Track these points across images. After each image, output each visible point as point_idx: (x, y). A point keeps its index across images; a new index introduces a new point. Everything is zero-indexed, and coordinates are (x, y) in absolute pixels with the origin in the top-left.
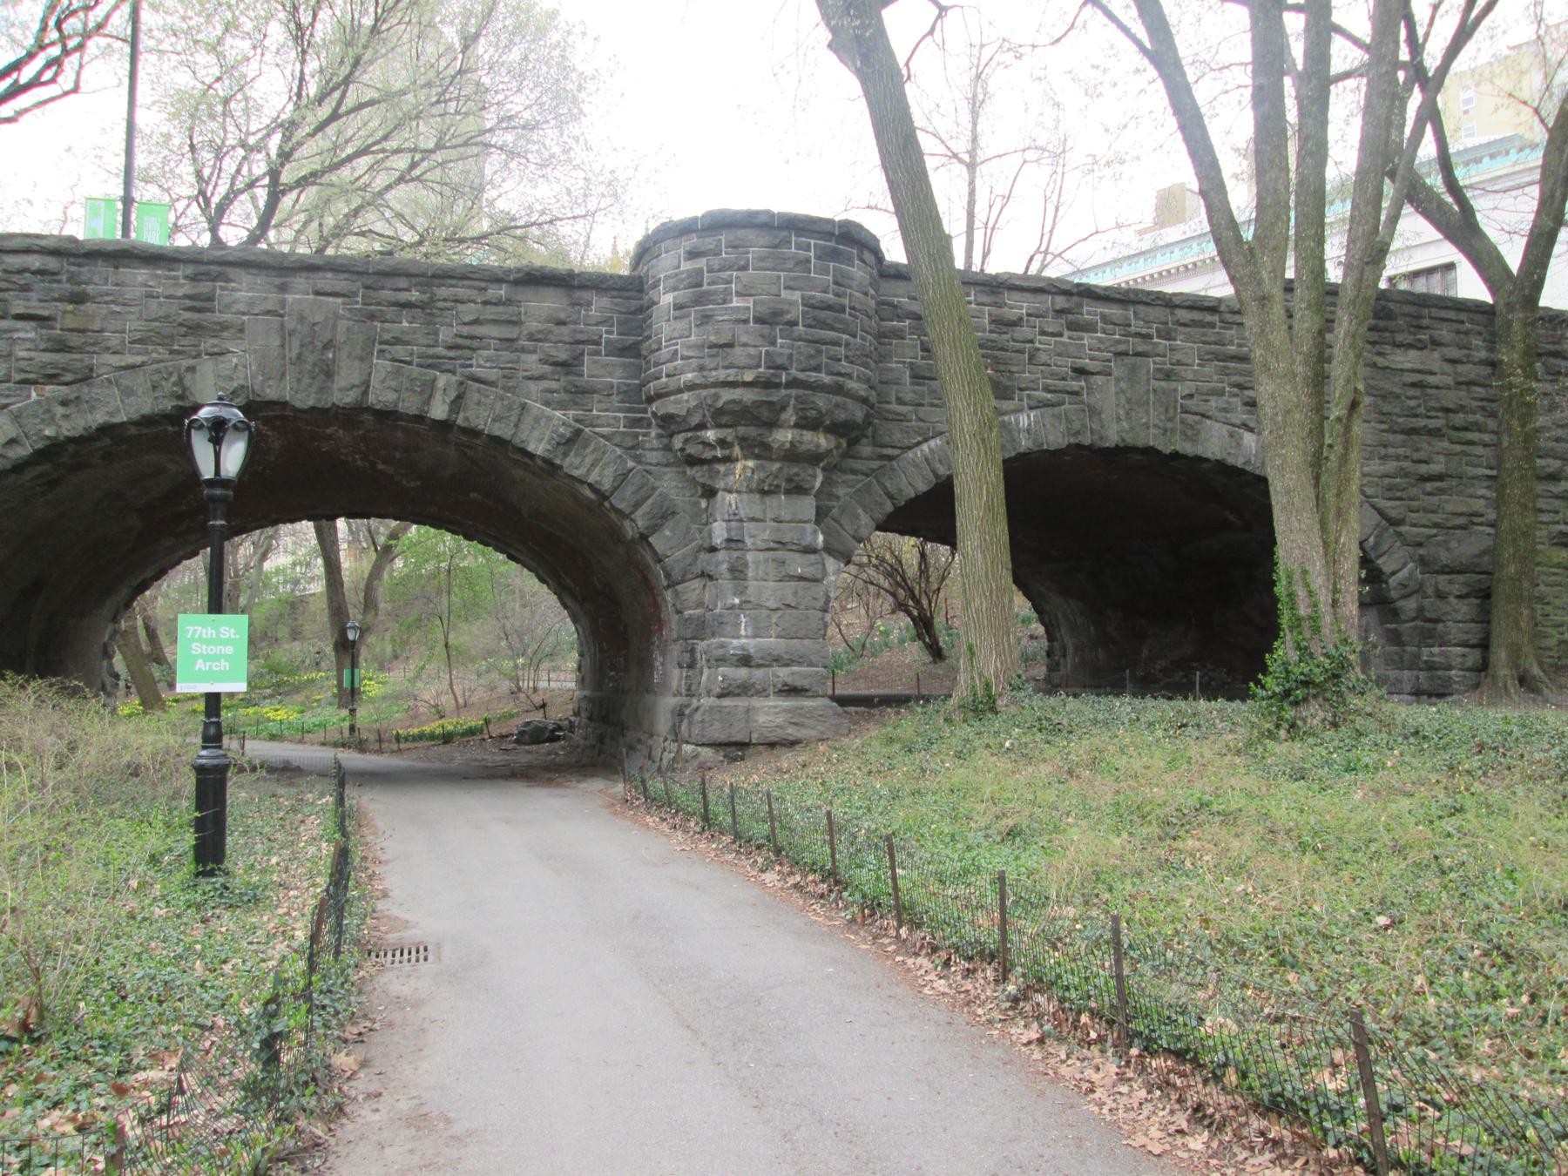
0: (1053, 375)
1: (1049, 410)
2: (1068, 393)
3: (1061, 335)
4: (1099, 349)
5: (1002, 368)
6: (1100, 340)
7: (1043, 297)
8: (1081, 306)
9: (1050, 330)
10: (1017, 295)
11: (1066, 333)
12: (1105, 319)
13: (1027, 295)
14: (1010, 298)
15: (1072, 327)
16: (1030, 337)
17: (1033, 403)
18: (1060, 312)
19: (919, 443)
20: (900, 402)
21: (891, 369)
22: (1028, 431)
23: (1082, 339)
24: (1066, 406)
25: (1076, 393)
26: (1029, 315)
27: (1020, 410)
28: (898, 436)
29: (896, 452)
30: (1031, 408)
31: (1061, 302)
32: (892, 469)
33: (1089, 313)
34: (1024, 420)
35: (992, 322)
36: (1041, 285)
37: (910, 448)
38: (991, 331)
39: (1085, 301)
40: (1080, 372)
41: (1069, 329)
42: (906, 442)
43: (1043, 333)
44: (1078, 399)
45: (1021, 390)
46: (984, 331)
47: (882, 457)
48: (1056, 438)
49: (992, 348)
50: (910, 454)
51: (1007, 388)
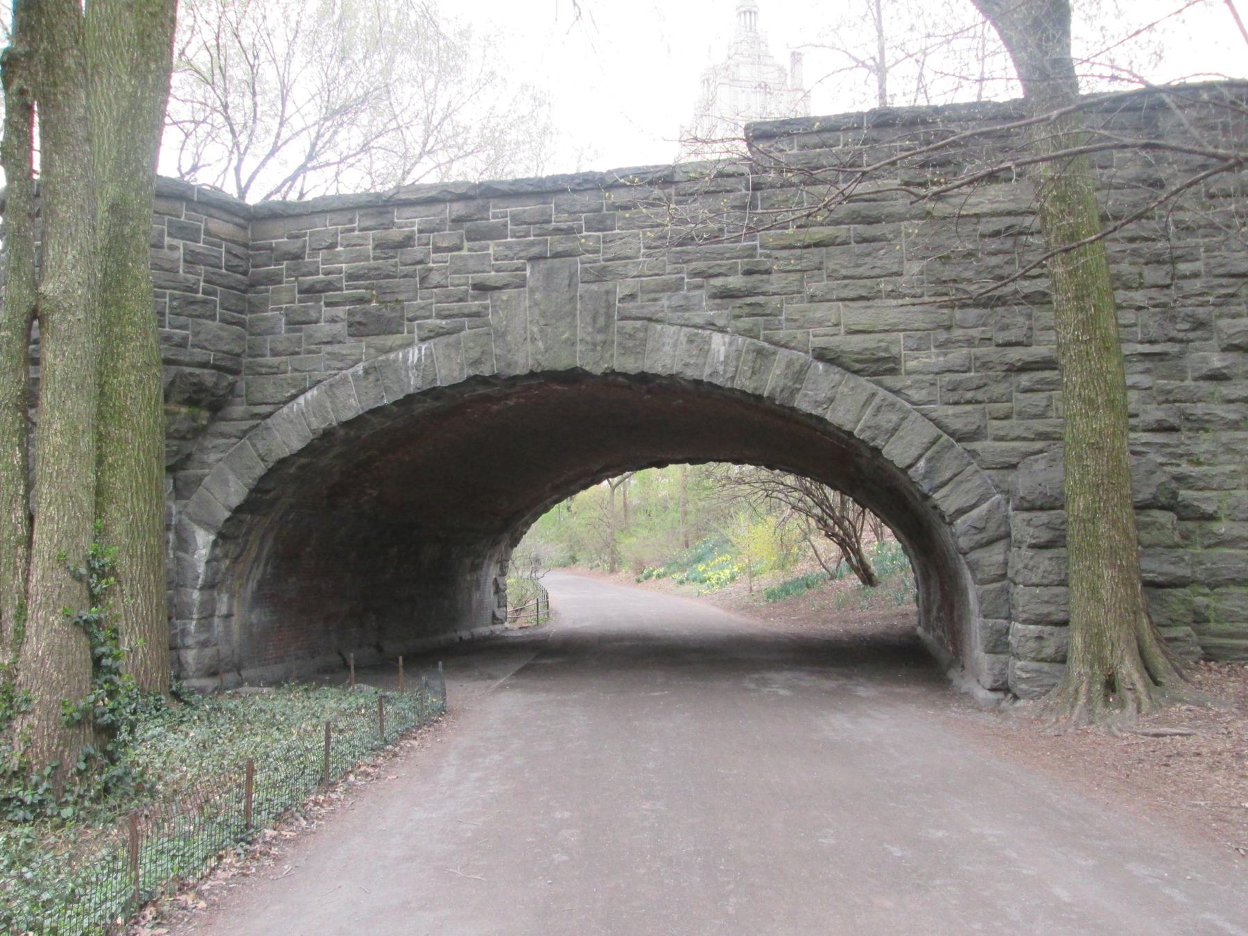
0: (448, 298)
1: (444, 339)
2: (468, 316)
3: (460, 248)
4: (506, 257)
5: (388, 298)
6: (509, 247)
7: (438, 208)
8: (488, 210)
9: (445, 245)
10: (408, 212)
11: (466, 244)
12: (517, 220)
13: (419, 208)
14: (399, 216)
15: (473, 236)
16: (420, 256)
17: (425, 334)
18: (458, 221)
19: (294, 397)
20: (275, 353)
21: (266, 319)
22: (417, 367)
23: (487, 248)
24: (467, 332)
25: (477, 315)
26: (420, 231)
27: (410, 344)
28: (270, 390)
29: (268, 409)
30: (423, 340)
31: (458, 209)
32: (268, 429)
33: (495, 217)
34: (413, 355)
35: (376, 247)
36: (433, 193)
37: (285, 403)
38: (375, 258)
39: (492, 202)
40: (482, 288)
41: (469, 239)
42: (279, 397)
43: (437, 250)
44: (479, 321)
45: (410, 320)
46: (367, 259)
47: (254, 416)
48: (450, 372)
49: (377, 277)
50: (285, 410)
51: (389, 321)
